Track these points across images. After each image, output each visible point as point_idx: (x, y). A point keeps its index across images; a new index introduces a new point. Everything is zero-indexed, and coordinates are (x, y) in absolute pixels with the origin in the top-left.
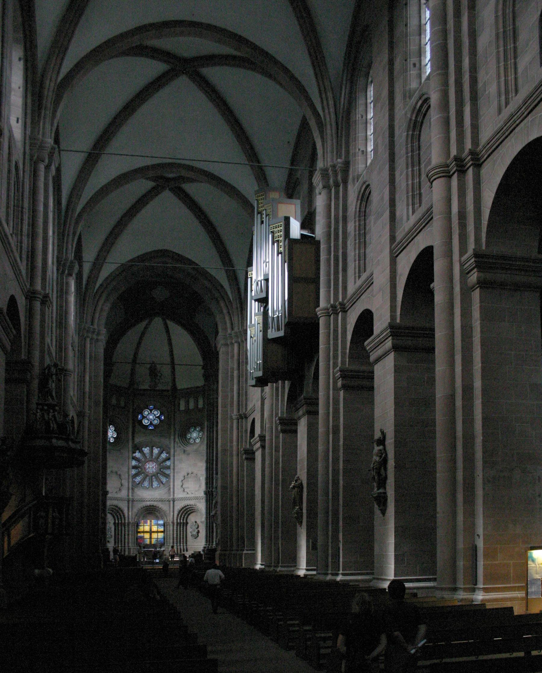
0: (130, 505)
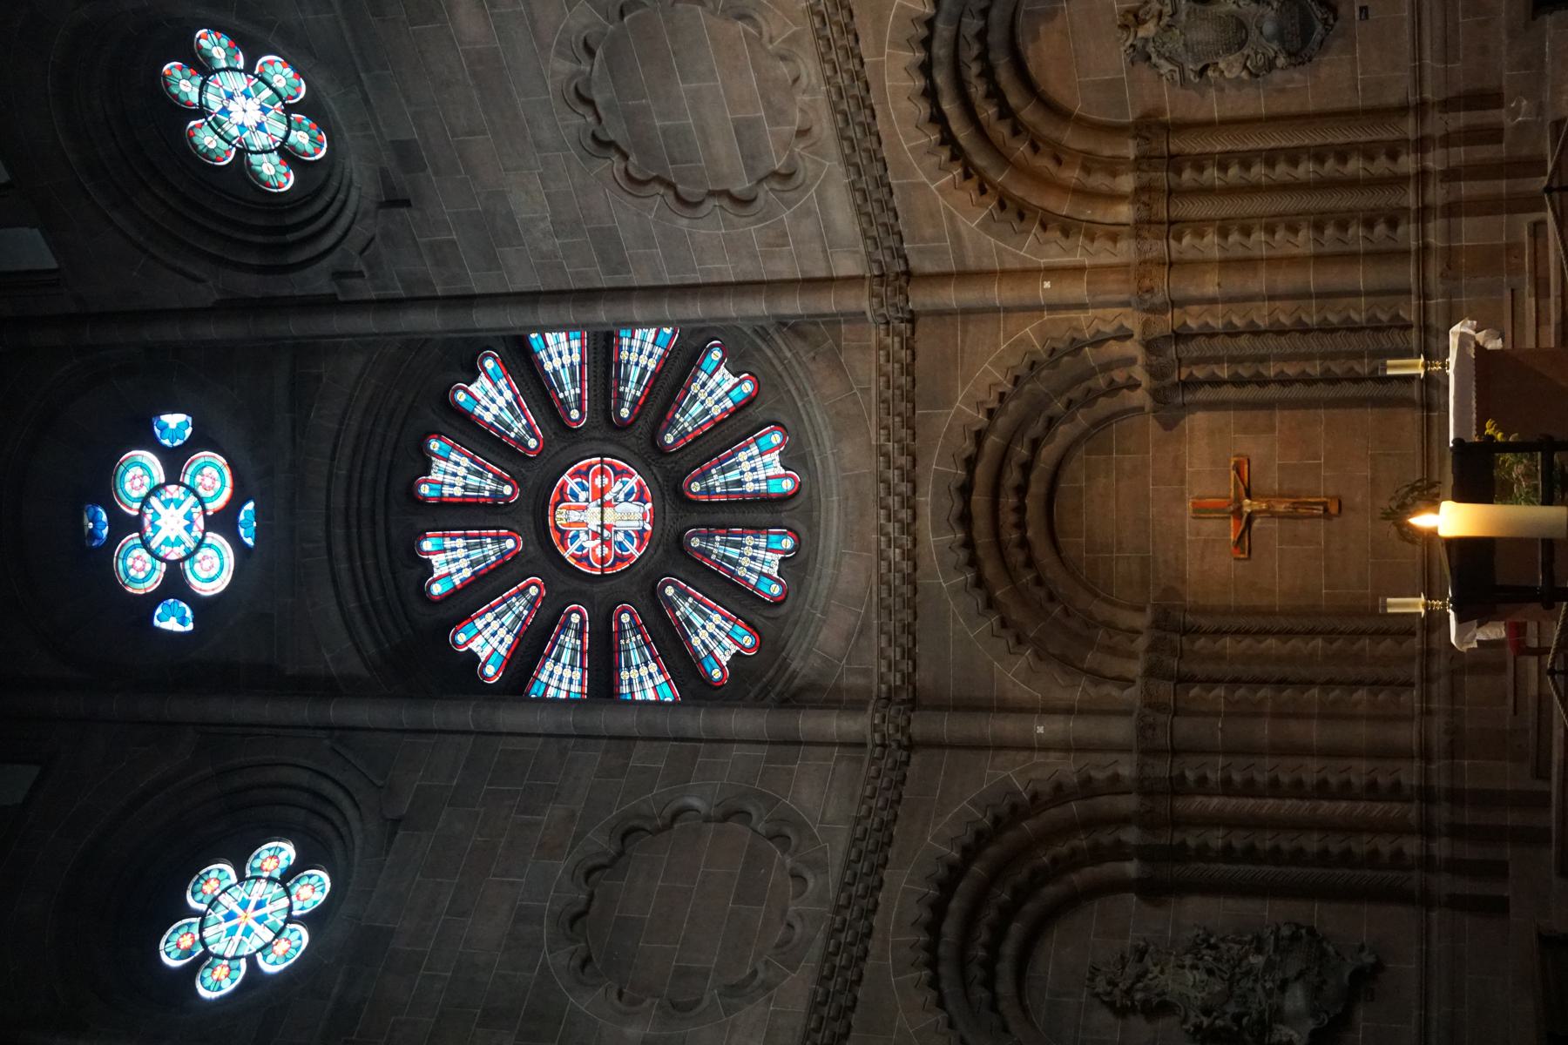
0: (946, 726)
